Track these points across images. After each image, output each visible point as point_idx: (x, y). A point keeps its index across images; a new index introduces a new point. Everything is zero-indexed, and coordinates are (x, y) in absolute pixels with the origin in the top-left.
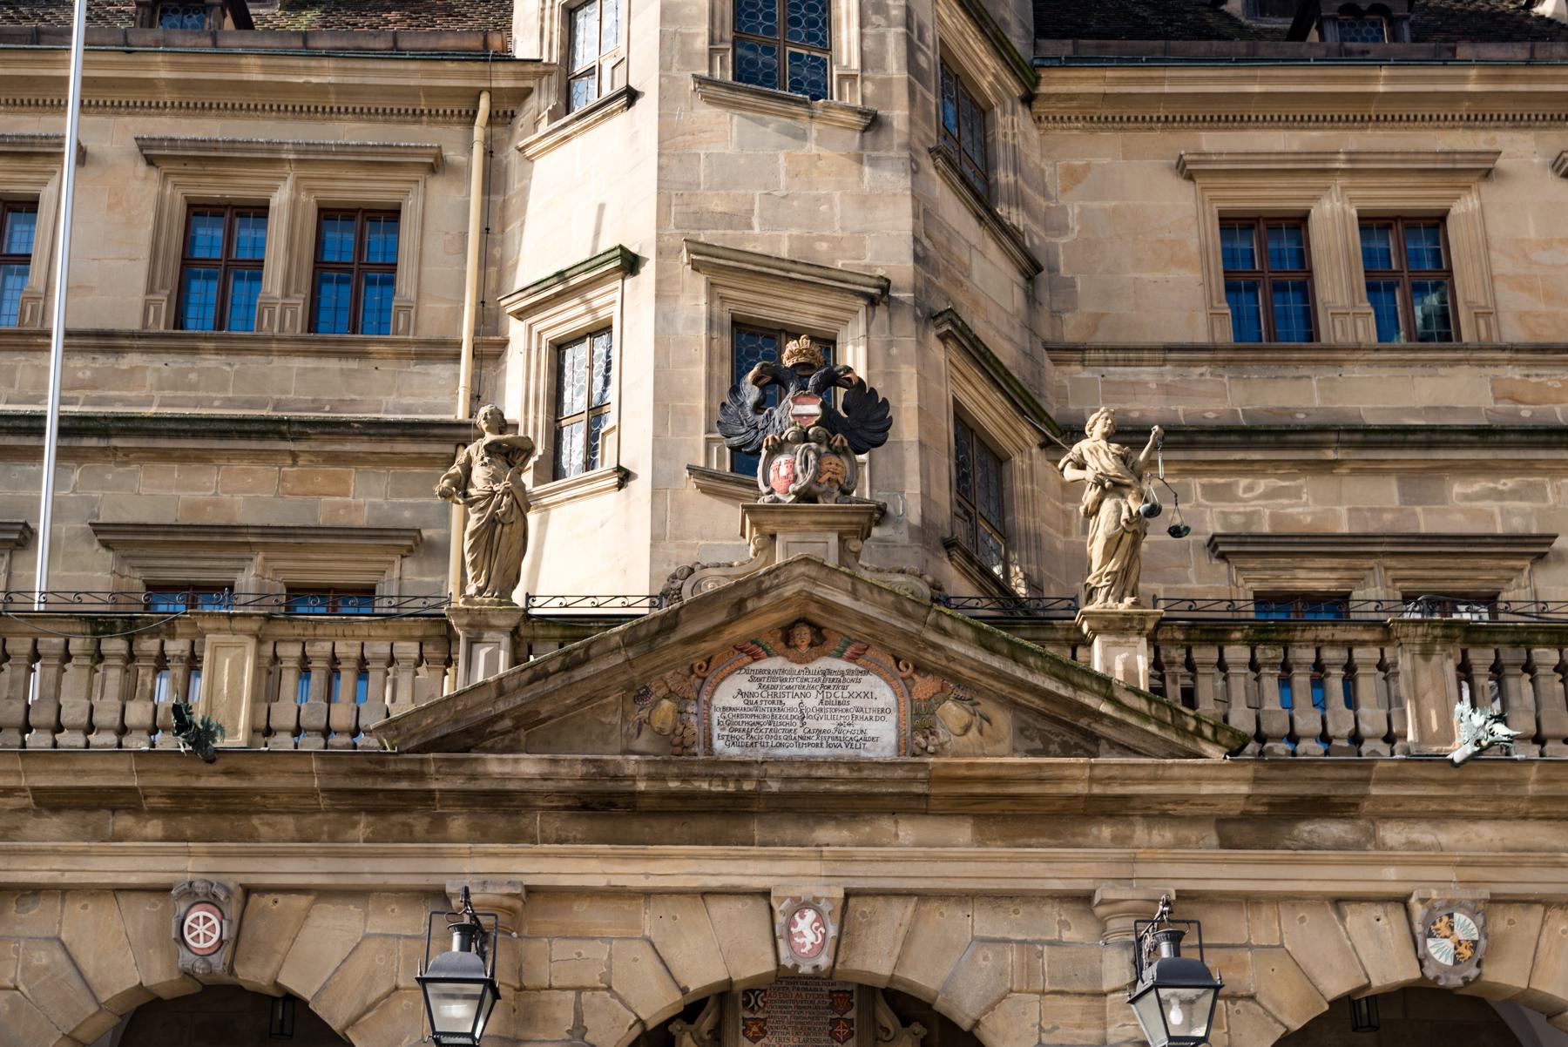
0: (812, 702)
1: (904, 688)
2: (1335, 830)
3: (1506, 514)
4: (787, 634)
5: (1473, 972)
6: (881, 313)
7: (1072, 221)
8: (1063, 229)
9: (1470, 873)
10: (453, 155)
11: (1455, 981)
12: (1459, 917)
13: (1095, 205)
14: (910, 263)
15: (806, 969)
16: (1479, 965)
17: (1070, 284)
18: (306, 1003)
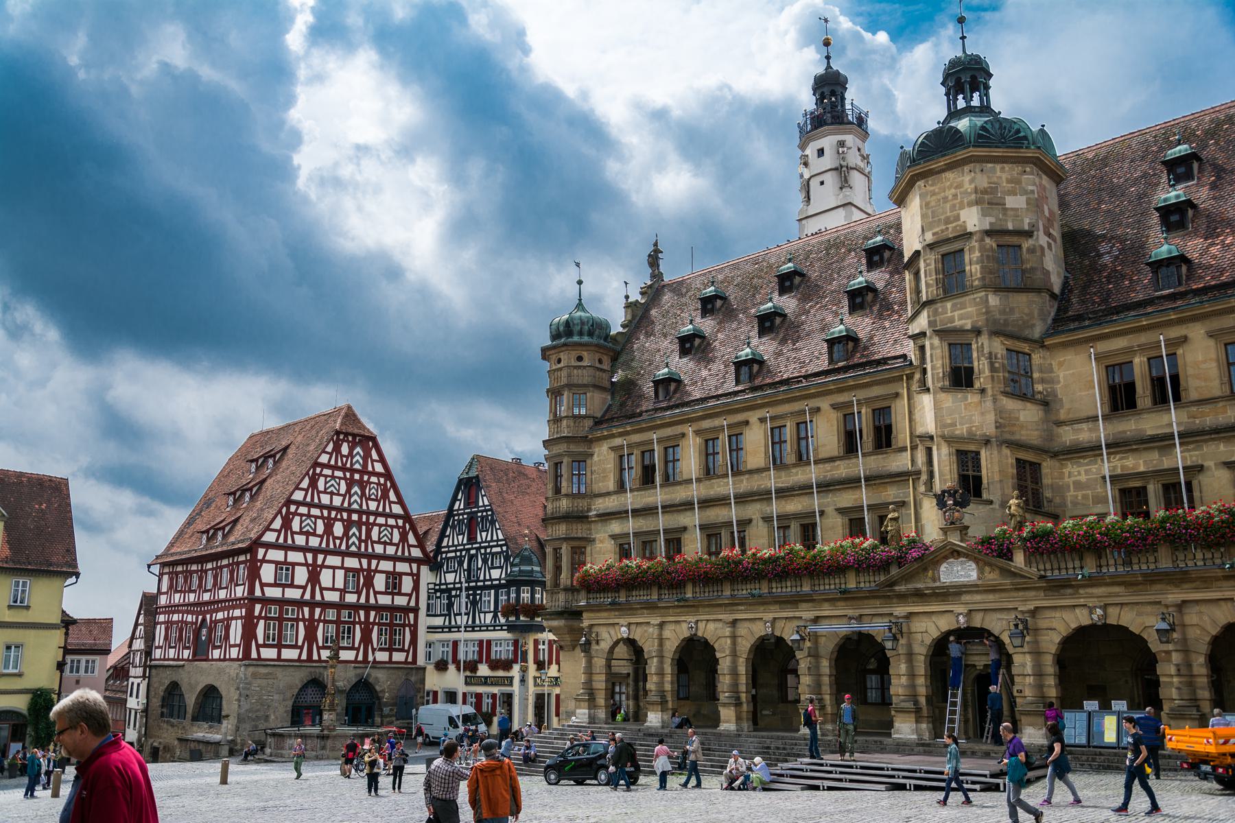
0: (959, 568)
1: (977, 564)
2: (1069, 591)
3: (1191, 456)
4: (952, 553)
5: (1103, 622)
6: (989, 446)
7: (1062, 380)
8: (1059, 382)
9: (1100, 599)
10: (900, 391)
11: (1100, 623)
12: (1097, 610)
13: (1067, 372)
14: (994, 430)
15: (962, 627)
16: (1105, 619)
17: (1061, 400)
18: (873, 637)
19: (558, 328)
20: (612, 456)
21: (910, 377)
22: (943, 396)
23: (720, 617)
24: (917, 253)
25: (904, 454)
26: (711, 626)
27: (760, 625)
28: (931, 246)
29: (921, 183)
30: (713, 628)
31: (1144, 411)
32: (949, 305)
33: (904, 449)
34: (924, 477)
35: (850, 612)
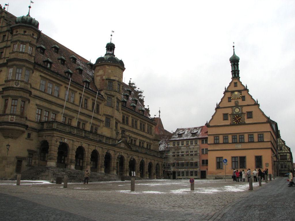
19: (35, 23)
20: (40, 78)
21: (104, 101)
22: (115, 110)
23: (89, 143)
24: (114, 80)
25: (101, 116)
26: (85, 145)
27: (95, 147)
28: (118, 81)
29: (118, 68)
30: (85, 145)
31: (125, 125)
32: (118, 94)
33: (101, 115)
34: (105, 123)
35: (109, 148)
